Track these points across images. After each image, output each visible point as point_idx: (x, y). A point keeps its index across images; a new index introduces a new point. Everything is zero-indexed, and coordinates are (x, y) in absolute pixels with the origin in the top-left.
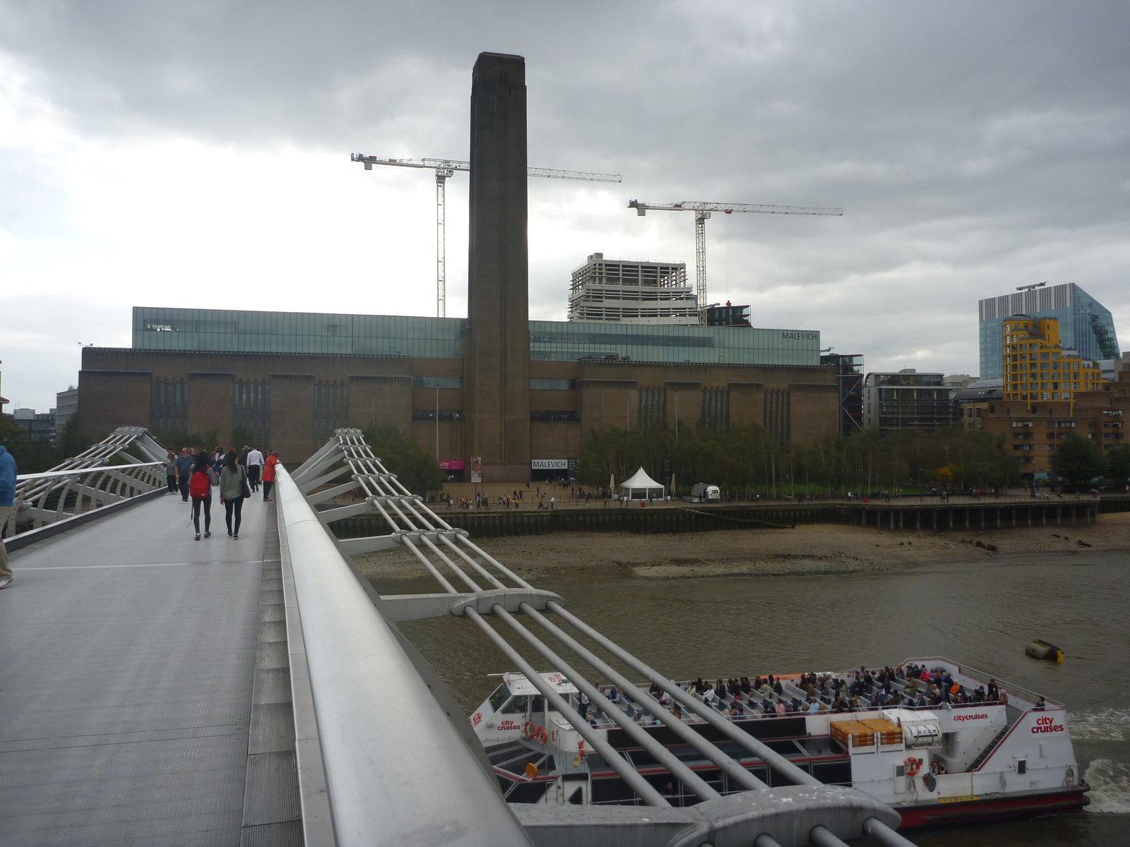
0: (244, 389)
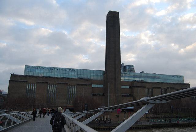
0: (50, 86)
